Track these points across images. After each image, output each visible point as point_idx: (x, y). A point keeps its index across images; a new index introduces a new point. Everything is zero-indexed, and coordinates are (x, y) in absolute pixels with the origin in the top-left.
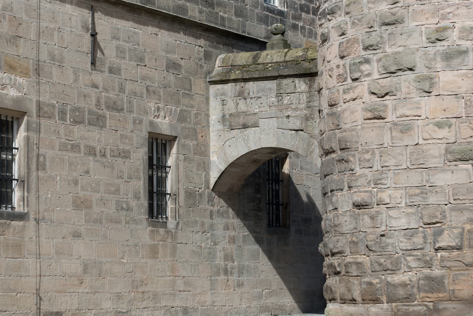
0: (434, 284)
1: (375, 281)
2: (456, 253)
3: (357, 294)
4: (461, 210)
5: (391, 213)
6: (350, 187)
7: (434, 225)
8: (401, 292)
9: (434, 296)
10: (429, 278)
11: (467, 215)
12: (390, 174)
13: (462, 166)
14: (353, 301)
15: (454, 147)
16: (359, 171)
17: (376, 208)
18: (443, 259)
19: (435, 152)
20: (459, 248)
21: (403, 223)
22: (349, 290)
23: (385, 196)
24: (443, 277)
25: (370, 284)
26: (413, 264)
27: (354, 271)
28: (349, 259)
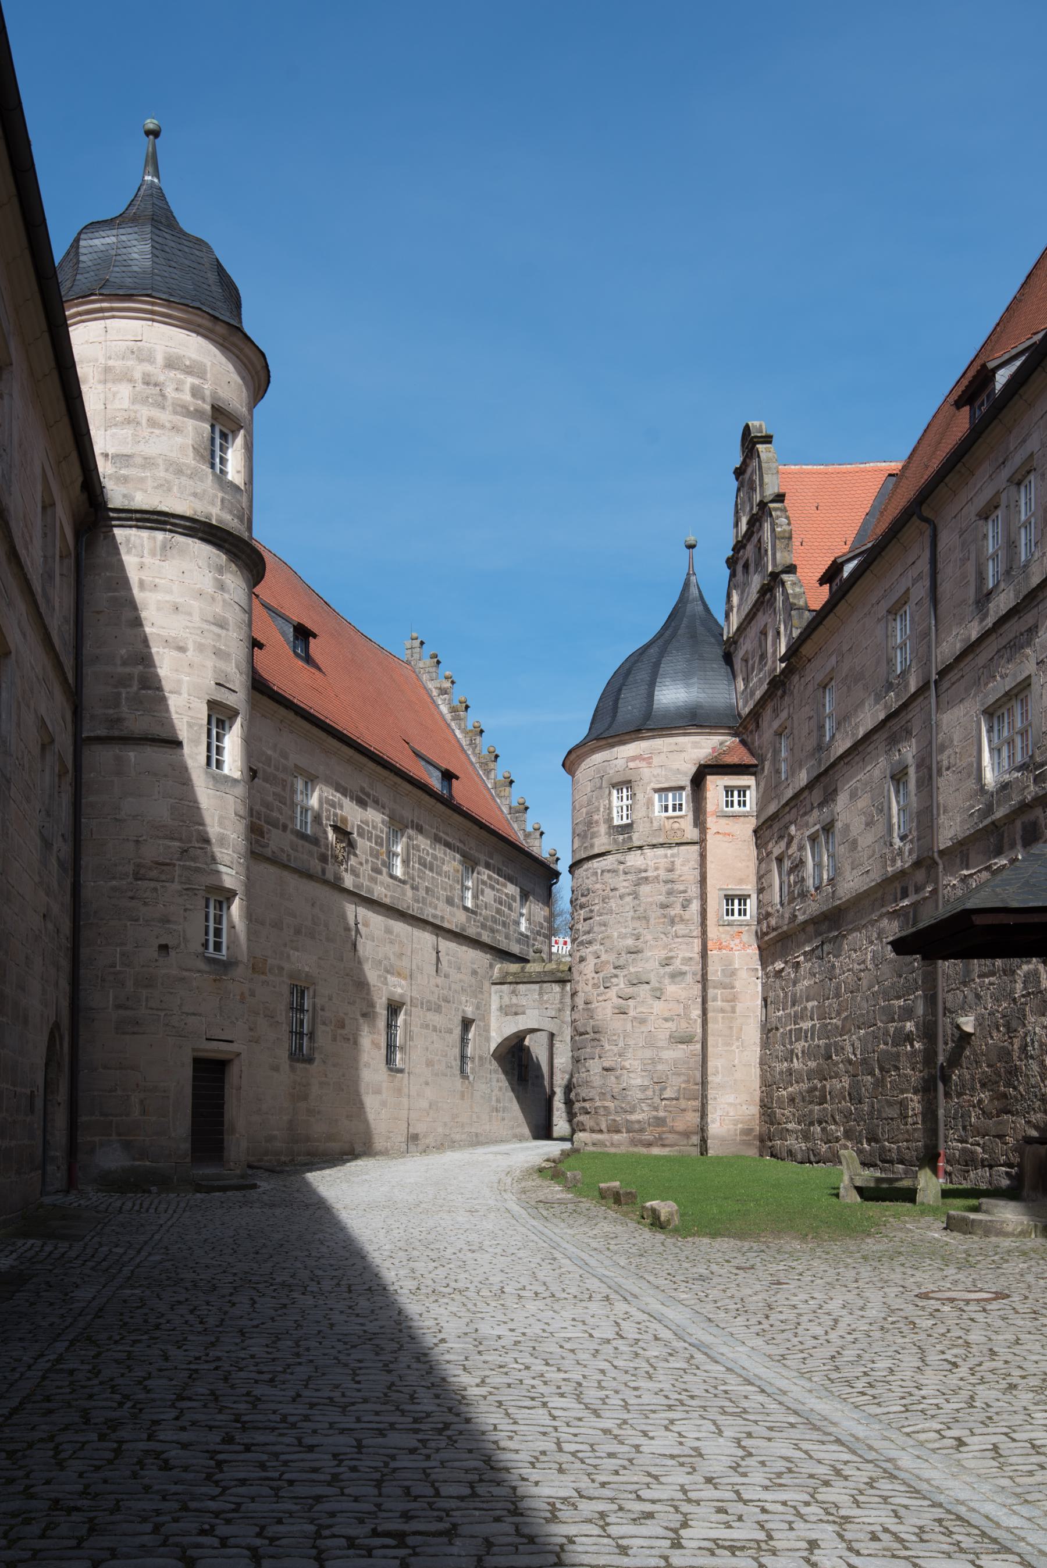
0: (660, 1122)
1: (618, 1119)
2: (675, 1102)
3: (604, 1127)
4: (679, 1075)
5: (631, 1075)
6: (600, 1057)
7: (661, 1084)
8: (637, 1126)
9: (659, 1129)
10: (656, 1118)
11: (683, 1078)
12: (630, 1050)
13: (681, 1046)
14: (601, 1131)
15: (675, 1034)
16: (607, 1047)
17: (619, 1072)
18: (665, 1106)
19: (663, 1036)
20: (677, 1099)
21: (639, 1081)
22: (598, 1124)
23: (627, 1064)
24: (665, 1117)
25: (615, 1120)
26: (645, 1109)
27: (601, 1111)
28: (597, 1104)
